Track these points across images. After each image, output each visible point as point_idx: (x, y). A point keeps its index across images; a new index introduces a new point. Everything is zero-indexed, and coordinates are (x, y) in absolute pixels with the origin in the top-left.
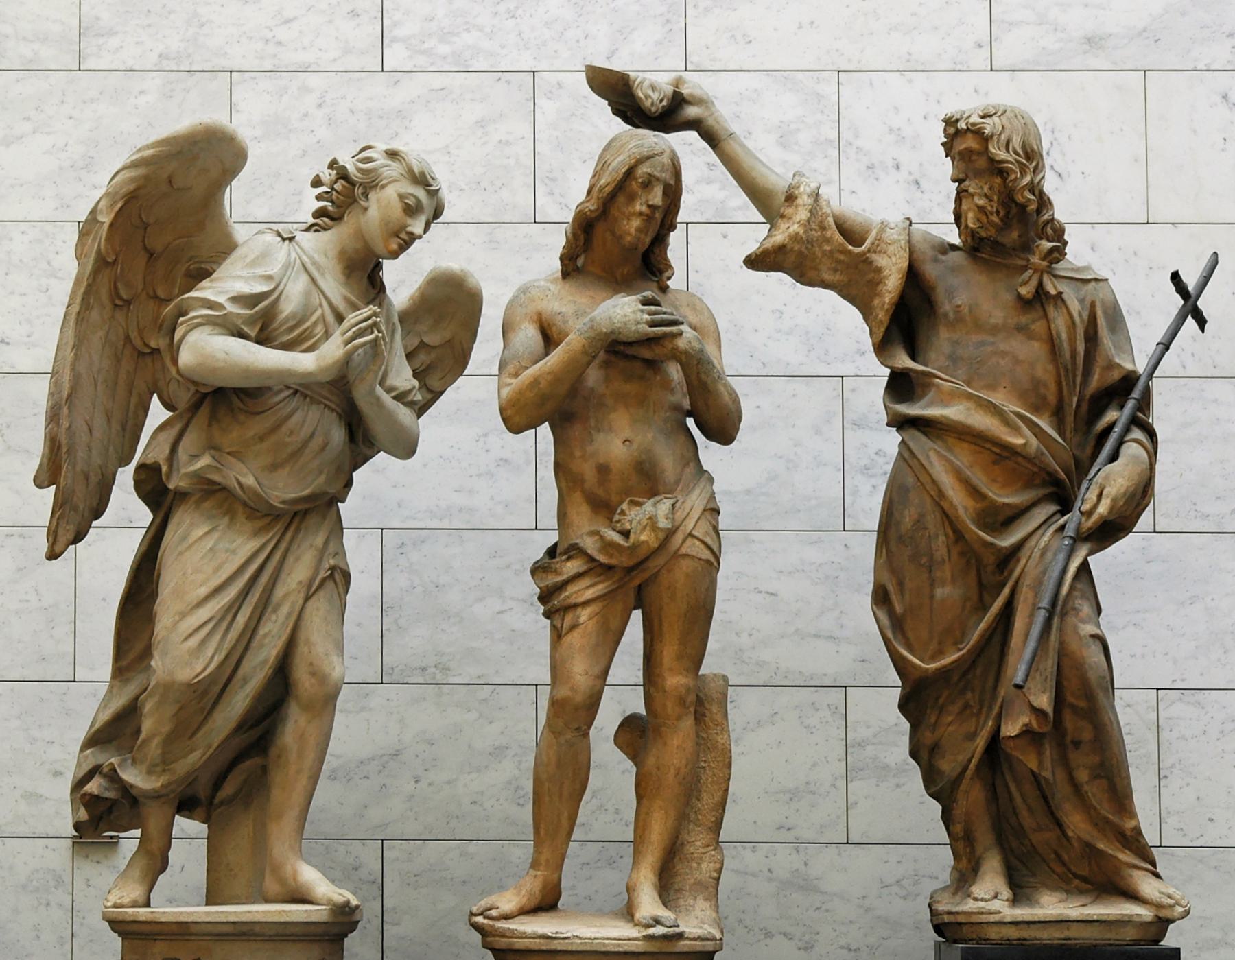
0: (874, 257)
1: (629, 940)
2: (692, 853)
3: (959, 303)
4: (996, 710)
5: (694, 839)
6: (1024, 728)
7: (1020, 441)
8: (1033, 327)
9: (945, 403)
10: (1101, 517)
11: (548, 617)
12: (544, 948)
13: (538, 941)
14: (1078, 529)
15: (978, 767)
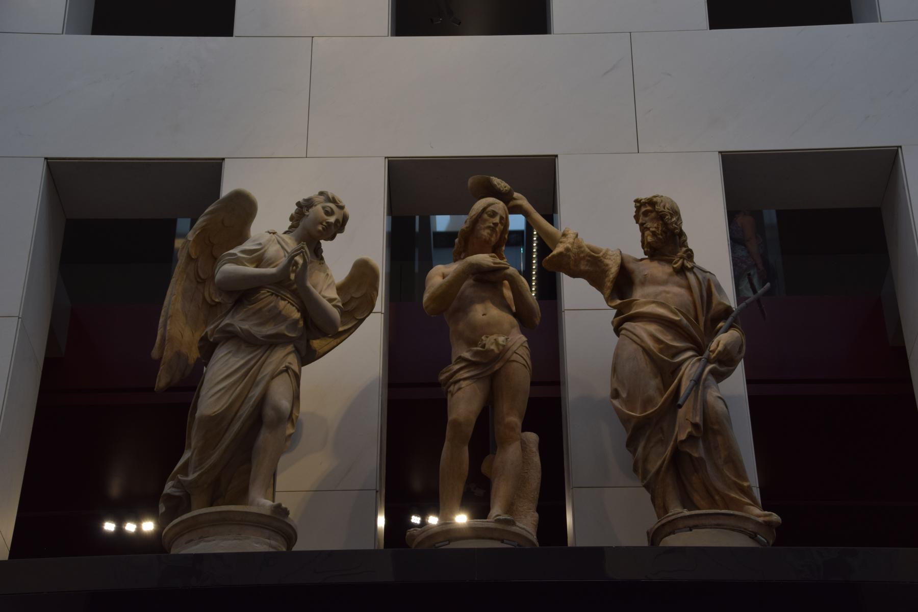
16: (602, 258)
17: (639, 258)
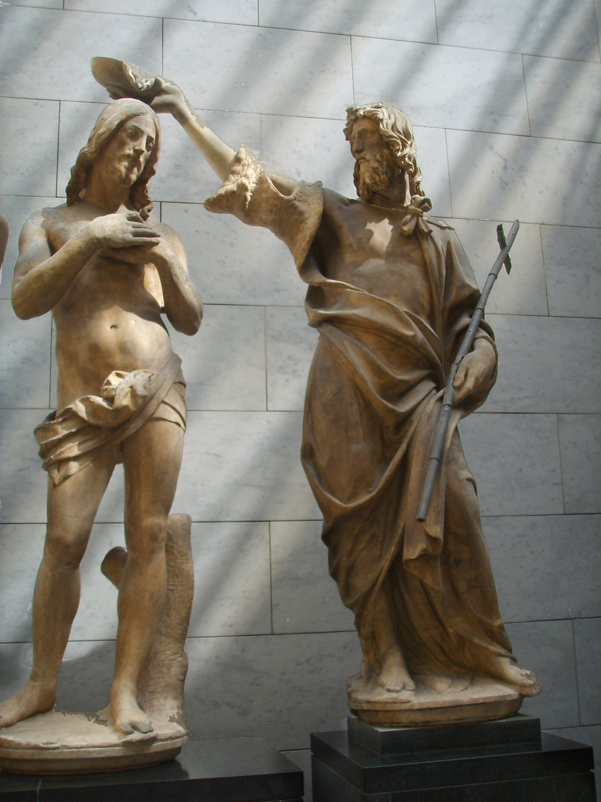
0: (297, 203)
1: (111, 746)
2: (163, 661)
3: (360, 236)
4: (397, 538)
5: (164, 649)
6: (423, 553)
7: (410, 333)
9: (355, 307)
10: (469, 391)
11: (46, 470)
12: (37, 757)
13: (31, 751)
14: (453, 400)
15: (383, 585)
16: (294, 202)
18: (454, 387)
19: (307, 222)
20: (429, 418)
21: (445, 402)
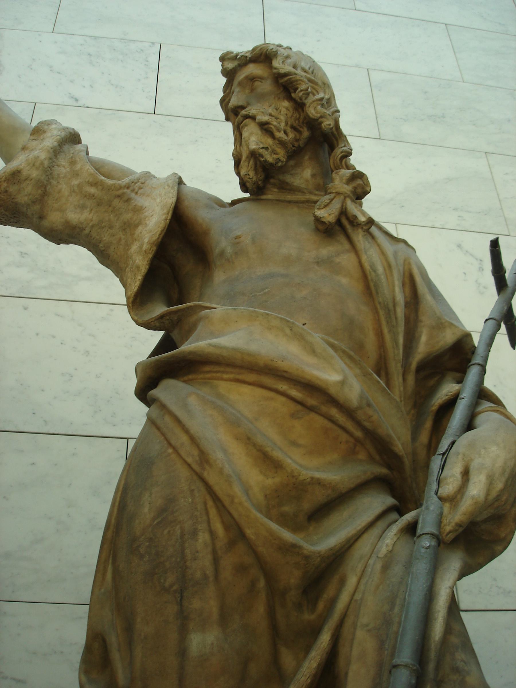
8: (337, 260)
17: (228, 200)
18: (440, 498)
19: (148, 222)
20: (386, 568)
21: (422, 528)
